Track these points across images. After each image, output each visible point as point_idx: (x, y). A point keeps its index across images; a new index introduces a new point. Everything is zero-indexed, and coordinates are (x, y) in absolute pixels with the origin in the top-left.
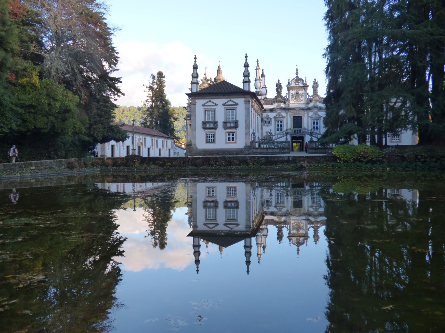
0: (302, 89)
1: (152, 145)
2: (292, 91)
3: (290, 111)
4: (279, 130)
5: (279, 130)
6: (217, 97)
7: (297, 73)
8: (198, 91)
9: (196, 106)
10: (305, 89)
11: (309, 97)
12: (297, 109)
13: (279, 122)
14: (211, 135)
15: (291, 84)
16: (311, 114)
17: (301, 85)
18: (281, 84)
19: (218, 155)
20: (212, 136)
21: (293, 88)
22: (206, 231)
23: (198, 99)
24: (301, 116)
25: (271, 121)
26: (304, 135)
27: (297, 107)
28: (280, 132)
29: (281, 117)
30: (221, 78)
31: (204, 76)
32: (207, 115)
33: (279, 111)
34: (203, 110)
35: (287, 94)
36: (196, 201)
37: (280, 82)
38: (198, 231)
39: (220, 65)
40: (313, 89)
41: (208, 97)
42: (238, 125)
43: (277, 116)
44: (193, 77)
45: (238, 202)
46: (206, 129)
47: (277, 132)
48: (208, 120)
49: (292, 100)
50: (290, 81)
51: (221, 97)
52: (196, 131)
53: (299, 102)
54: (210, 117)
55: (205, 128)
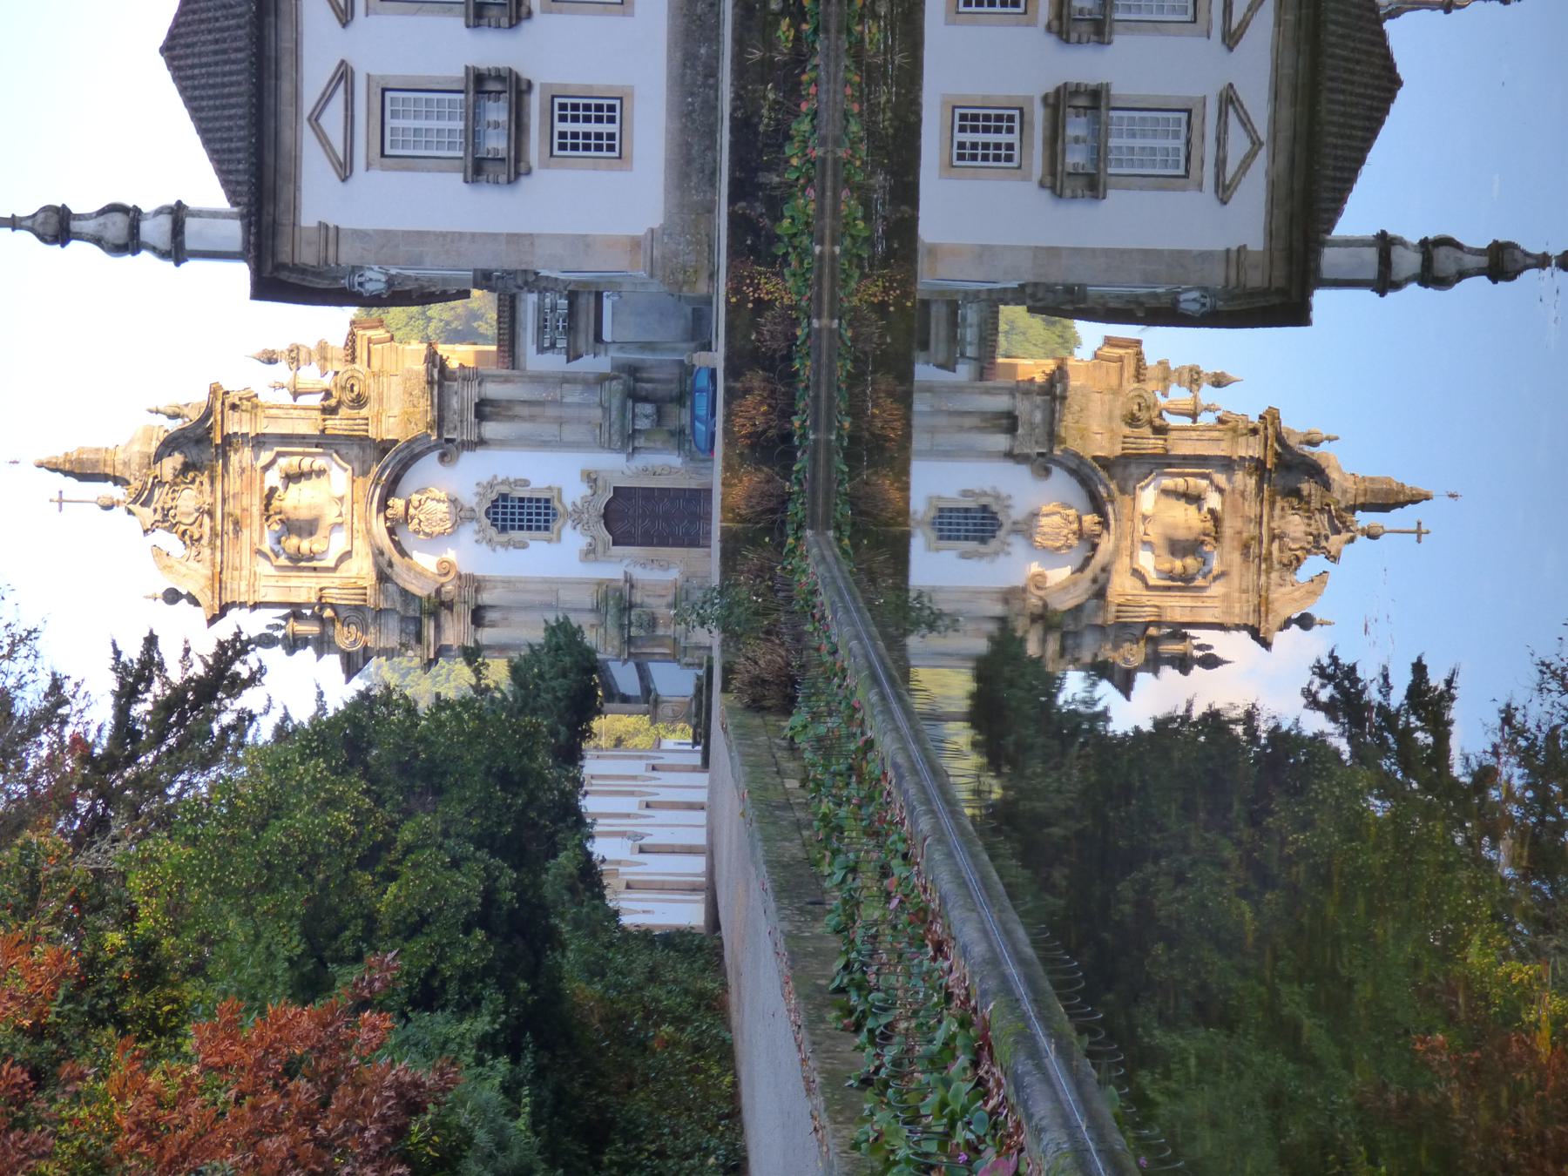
1: (622, 834)
6: (286, 65)
8: (236, 210)
9: (345, 224)
14: (569, 127)
19: (712, 72)
20: (575, 119)
22: (1272, 185)
23: (295, 208)
30: (136, 448)
31: (119, 511)
32: (416, 145)
34: (377, 175)
36: (1054, 252)
38: (1270, 249)
39: (44, 458)
41: (286, 135)
42: (499, 76)
44: (130, 244)
45: (1058, 91)
46: (518, 160)
48: (451, 145)
51: (286, 33)
52: (531, 235)
54: (434, 124)
55: (514, 167)
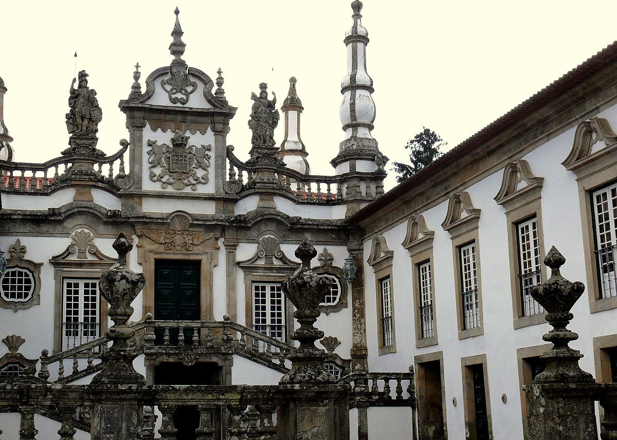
0: (202, 127)
2: (154, 130)
3: (138, 228)
4: (81, 329)
5: (81, 329)
7: (177, 48)
10: (219, 127)
11: (235, 169)
12: (178, 226)
13: (81, 289)
15: (149, 94)
16: (246, 251)
17: (197, 101)
18: (93, 92)
21: (159, 117)
24: (198, 263)
25: (38, 281)
26: (227, 356)
27: (180, 215)
28: (81, 340)
29: (90, 258)
33: (79, 228)
35: (124, 144)
37: (91, 85)
40: (250, 133)
43: (68, 252)
47: (69, 343)
49: (152, 176)
50: (142, 82)
53: (188, 190)
